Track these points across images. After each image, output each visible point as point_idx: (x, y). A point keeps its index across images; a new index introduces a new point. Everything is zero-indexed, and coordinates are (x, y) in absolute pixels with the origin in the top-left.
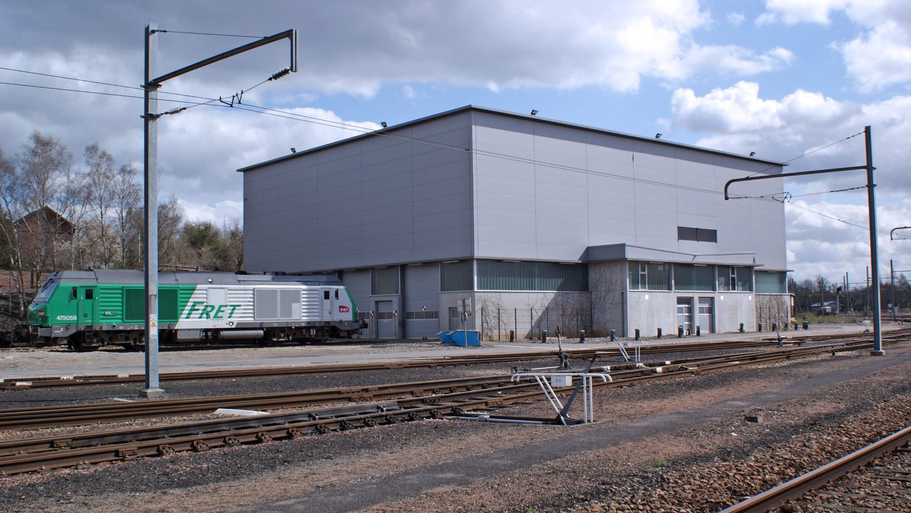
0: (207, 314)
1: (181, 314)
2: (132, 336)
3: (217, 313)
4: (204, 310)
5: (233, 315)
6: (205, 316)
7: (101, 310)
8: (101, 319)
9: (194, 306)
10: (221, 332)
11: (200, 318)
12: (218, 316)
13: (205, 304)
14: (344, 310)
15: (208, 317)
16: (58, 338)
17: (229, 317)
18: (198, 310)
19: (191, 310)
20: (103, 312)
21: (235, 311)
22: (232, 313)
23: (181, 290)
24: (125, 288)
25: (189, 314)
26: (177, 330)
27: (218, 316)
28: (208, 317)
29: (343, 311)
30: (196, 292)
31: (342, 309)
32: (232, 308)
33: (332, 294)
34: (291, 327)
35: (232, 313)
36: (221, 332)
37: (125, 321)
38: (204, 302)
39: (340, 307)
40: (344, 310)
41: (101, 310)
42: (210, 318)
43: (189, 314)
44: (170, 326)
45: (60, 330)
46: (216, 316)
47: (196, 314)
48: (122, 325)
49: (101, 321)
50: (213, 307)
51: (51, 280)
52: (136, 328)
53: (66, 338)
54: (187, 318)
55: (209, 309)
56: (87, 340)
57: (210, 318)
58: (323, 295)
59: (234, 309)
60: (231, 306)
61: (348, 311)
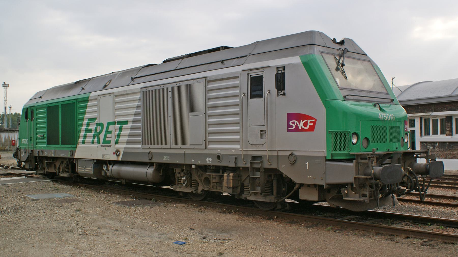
3: (105, 137)
4: (96, 130)
5: (121, 139)
9: (88, 125)
11: (93, 142)
12: (107, 139)
13: (97, 121)
14: (301, 125)
17: (117, 142)
18: (90, 131)
21: (123, 132)
22: (119, 136)
25: (85, 137)
28: (99, 142)
29: (297, 129)
30: (89, 104)
31: (294, 123)
34: (190, 166)
35: (119, 136)
39: (291, 117)
40: (301, 125)
43: (85, 137)
46: (105, 142)
54: (84, 142)
59: (121, 129)
60: (119, 123)
61: (312, 129)
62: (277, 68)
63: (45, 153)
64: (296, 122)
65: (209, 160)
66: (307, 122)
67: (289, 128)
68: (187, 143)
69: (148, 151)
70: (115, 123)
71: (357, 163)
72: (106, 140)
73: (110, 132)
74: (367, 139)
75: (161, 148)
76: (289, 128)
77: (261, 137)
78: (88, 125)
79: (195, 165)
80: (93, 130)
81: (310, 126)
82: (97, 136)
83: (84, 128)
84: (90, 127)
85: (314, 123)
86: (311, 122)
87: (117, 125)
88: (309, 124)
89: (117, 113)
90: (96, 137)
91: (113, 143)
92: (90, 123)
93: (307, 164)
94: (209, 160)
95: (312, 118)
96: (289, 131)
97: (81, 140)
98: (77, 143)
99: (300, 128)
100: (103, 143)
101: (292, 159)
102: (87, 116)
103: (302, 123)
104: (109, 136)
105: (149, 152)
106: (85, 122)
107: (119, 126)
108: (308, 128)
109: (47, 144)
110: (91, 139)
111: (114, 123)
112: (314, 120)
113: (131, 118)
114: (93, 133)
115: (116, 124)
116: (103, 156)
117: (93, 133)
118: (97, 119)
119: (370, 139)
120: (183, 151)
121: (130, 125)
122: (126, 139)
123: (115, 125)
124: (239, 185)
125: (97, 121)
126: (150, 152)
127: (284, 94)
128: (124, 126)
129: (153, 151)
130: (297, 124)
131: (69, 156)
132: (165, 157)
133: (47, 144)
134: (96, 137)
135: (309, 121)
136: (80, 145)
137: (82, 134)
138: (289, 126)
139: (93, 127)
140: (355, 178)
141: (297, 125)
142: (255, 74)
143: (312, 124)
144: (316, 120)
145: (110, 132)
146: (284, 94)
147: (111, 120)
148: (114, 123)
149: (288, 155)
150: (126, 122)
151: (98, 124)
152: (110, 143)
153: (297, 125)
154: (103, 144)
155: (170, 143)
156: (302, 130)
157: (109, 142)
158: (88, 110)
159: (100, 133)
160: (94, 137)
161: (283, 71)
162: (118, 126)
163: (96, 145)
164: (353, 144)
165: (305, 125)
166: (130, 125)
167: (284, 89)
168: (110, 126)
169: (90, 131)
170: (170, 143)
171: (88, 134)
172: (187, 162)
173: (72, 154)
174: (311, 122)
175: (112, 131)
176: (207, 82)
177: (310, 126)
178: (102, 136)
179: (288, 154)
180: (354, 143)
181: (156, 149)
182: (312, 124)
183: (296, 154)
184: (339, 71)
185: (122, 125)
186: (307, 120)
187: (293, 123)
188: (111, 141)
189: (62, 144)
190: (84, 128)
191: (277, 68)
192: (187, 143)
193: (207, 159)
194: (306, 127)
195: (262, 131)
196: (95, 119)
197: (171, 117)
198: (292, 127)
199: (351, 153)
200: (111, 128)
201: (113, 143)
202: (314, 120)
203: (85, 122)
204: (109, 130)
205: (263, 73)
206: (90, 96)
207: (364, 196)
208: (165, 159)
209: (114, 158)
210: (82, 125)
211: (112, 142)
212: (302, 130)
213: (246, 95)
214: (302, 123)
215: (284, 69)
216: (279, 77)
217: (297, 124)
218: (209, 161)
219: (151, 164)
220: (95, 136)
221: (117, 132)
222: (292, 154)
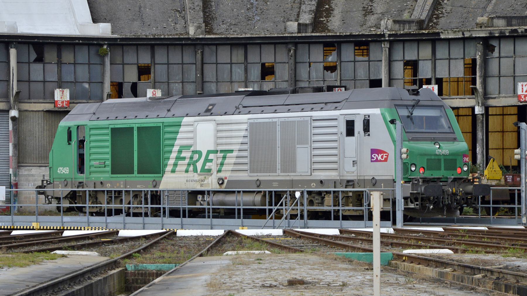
3: (204, 164)
4: (191, 158)
5: (224, 168)
9: (180, 152)
11: (187, 171)
12: (206, 168)
13: (192, 149)
17: (219, 171)
18: (184, 158)
21: (226, 161)
22: (222, 164)
25: (175, 165)
27: (206, 168)
28: (195, 170)
29: (377, 160)
31: (375, 156)
33: (359, 127)
35: (222, 164)
38: (191, 146)
39: (373, 151)
40: (379, 158)
43: (175, 165)
46: (203, 169)
47: (182, 166)
50: (200, 153)
54: (173, 171)
58: (343, 128)
59: (224, 158)
60: (222, 151)
61: (386, 160)
62: (365, 116)
63: (108, 185)
64: (376, 155)
66: (383, 155)
67: (372, 160)
68: (295, 171)
69: (256, 179)
70: (217, 151)
71: (413, 184)
73: (211, 161)
74: (424, 168)
75: (269, 176)
76: (372, 160)
77: (353, 166)
81: (385, 158)
82: (193, 165)
83: (174, 155)
84: (183, 155)
85: (387, 156)
86: (385, 156)
87: (220, 153)
88: (384, 157)
89: (220, 141)
90: (192, 166)
91: (214, 171)
92: (183, 151)
93: (382, 185)
94: (313, 185)
95: (386, 153)
96: (372, 161)
97: (169, 168)
98: (164, 172)
99: (379, 159)
100: (200, 172)
101: (374, 181)
103: (380, 156)
104: (208, 164)
105: (257, 179)
106: (176, 149)
107: (223, 154)
108: (384, 159)
109: (112, 173)
110: (184, 168)
112: (387, 154)
113: (237, 147)
115: (219, 152)
117: (187, 161)
118: (193, 146)
119: (426, 168)
122: (231, 168)
123: (217, 153)
124: (337, 204)
125: (192, 149)
126: (258, 180)
127: (369, 135)
128: (229, 155)
129: (260, 178)
130: (377, 157)
133: (112, 173)
134: (192, 166)
135: (385, 154)
137: (171, 162)
138: (372, 158)
139: (186, 154)
140: (411, 193)
141: (377, 158)
142: (350, 118)
143: (386, 157)
144: (388, 154)
145: (211, 161)
146: (369, 135)
147: (212, 148)
149: (371, 178)
150: (231, 151)
151: (194, 152)
152: (210, 172)
153: (377, 158)
155: (279, 172)
156: (380, 161)
157: (209, 170)
159: (197, 161)
160: (189, 165)
161: (368, 118)
164: (411, 170)
165: (382, 157)
166: (235, 154)
167: (369, 131)
168: (210, 154)
169: (184, 158)
170: (279, 172)
171: (180, 162)
173: (155, 185)
174: (385, 156)
175: (212, 160)
176: (312, 120)
177: (385, 158)
178: (199, 165)
179: (371, 178)
180: (413, 170)
181: (264, 177)
182: (386, 157)
183: (376, 178)
184: (409, 118)
185: (225, 154)
186: (383, 154)
187: (375, 156)
189: (138, 173)
190: (174, 155)
191: (365, 116)
192: (295, 171)
193: (312, 185)
194: (383, 159)
195: (353, 161)
196: (191, 146)
197: (280, 148)
198: (374, 158)
199: (409, 177)
200: (211, 156)
201: (214, 171)
202: (387, 154)
204: (209, 158)
205: (355, 118)
206: (183, 121)
207: (417, 205)
209: (217, 187)
210: (171, 152)
212: (380, 161)
213: (343, 133)
214: (380, 156)
215: (369, 117)
216: (365, 123)
217: (377, 157)
220: (190, 165)
221: (220, 161)
222: (373, 178)
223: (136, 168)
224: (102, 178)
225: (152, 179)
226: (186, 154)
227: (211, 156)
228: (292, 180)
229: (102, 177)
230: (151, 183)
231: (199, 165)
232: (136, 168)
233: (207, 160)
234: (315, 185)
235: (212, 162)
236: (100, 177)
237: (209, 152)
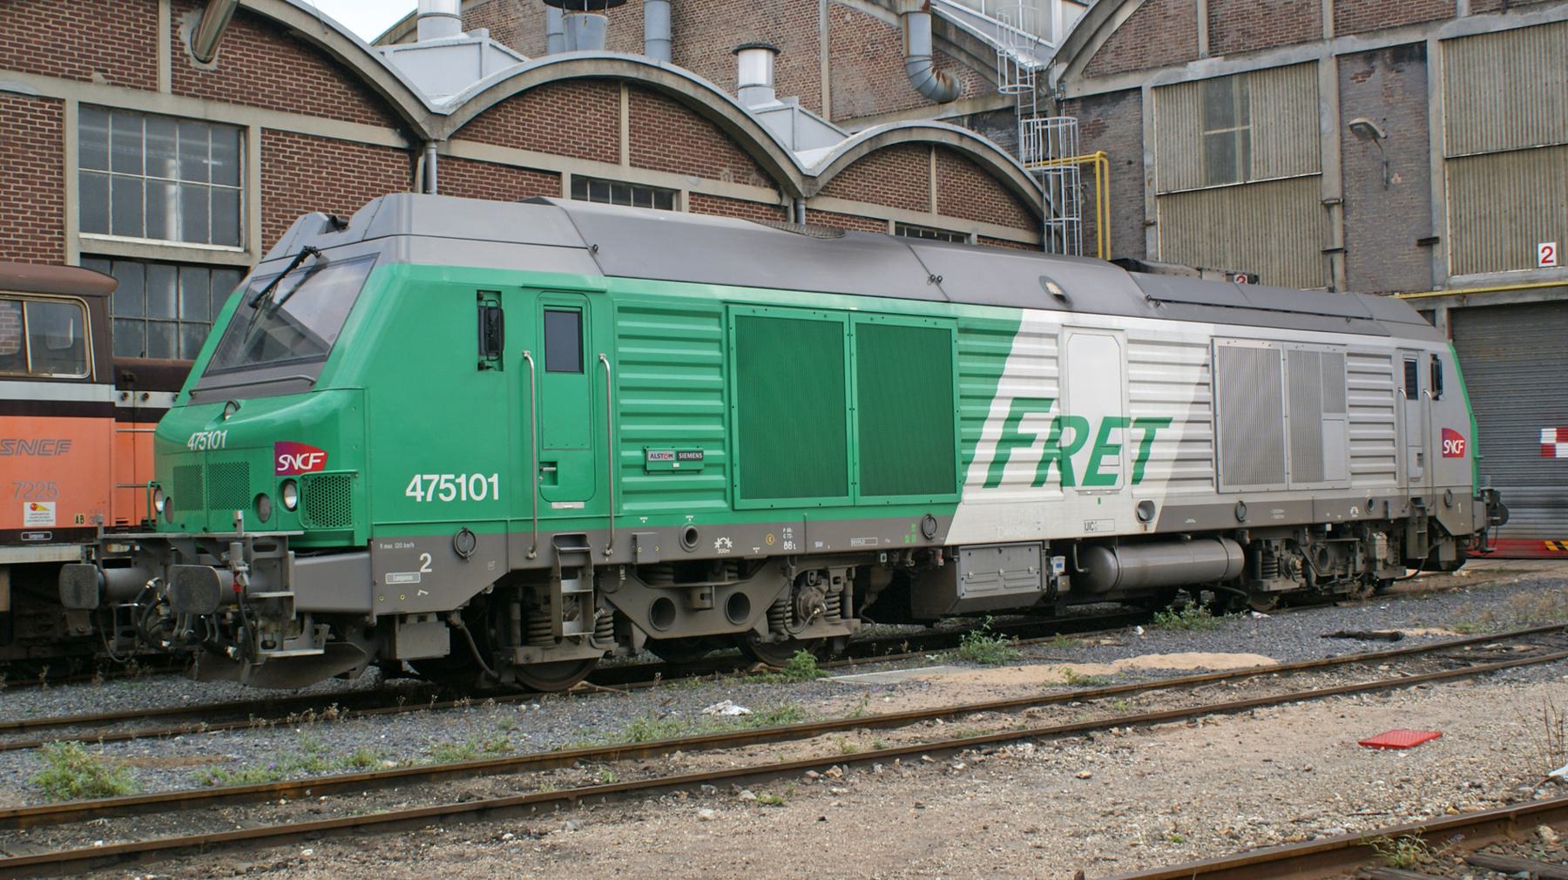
0: (1063, 465)
1: (967, 462)
2: (761, 593)
3: (1095, 462)
4: (1052, 441)
6: (1053, 472)
7: (629, 441)
8: (632, 493)
9: (1014, 419)
10: (1110, 558)
11: (1039, 482)
12: (1101, 471)
13: (1054, 411)
15: (1066, 480)
16: (403, 618)
17: (1137, 480)
18: (1028, 441)
19: (1007, 441)
20: (634, 454)
21: (1155, 450)
22: (1142, 460)
23: (965, 331)
24: (734, 310)
25: (999, 463)
26: (955, 548)
27: (1101, 471)
28: (1066, 480)
29: (1451, 455)
30: (1018, 345)
32: (1141, 432)
35: (1142, 460)
36: (1110, 558)
37: (741, 503)
40: (1454, 449)
41: (629, 441)
42: (1072, 484)
43: (999, 463)
44: (929, 528)
45: (415, 566)
46: (1092, 478)
48: (725, 531)
49: (626, 507)
50: (1081, 424)
51: (307, 252)
52: (788, 547)
53: (443, 616)
54: (992, 483)
55: (1069, 436)
56: (569, 629)
57: (1072, 484)
59: (1148, 441)
61: (1461, 455)
63: (718, 544)
65: (1354, 512)
72: (1099, 472)
73: (1115, 449)
75: (1268, 491)
78: (1014, 419)
79: (1332, 523)
80: (1040, 441)
83: (992, 430)
84: (1023, 429)
87: (1134, 427)
88: (1460, 447)
94: (1354, 512)
96: (1444, 455)
97: (976, 473)
100: (1083, 484)
102: (1005, 388)
103: (1455, 443)
104: (1105, 459)
106: (1000, 409)
110: (1031, 473)
111: (1123, 422)
114: (1037, 451)
115: (1132, 424)
116: (1088, 526)
117: (1037, 451)
118: (1055, 402)
120: (1308, 497)
121: (1176, 431)
122: (1167, 470)
125: (1054, 411)
128: (1161, 432)
129: (1247, 499)
131: (912, 539)
132: (1275, 511)
136: (968, 495)
137: (985, 452)
145: (1115, 449)
148: (1123, 422)
150: (1166, 422)
151: (1059, 422)
152: (1113, 484)
154: (1083, 484)
155: (1289, 478)
156: (1455, 455)
157: (1110, 479)
158: (1010, 366)
160: (1044, 463)
162: (1141, 432)
163: (1051, 492)
166: (1176, 431)
168: (1112, 429)
169: (1028, 441)
170: (1289, 478)
171: (1016, 452)
172: (1319, 520)
175: (1118, 447)
178: (1080, 462)
181: (1255, 495)
188: (1115, 476)
189: (865, 492)
190: (992, 430)
193: (1352, 511)
195: (1419, 455)
200: (1115, 436)
203: (1000, 409)
204: (1108, 442)
208: (1277, 517)
211: (1119, 481)
212: (1455, 455)
218: (1355, 513)
219: (1231, 534)
223: (854, 472)
224: (689, 517)
225: (921, 513)
226: (1037, 426)
227: (1115, 436)
228: (1313, 501)
229: (691, 511)
230: (914, 526)
231: (1080, 462)
232: (854, 472)
233: (1103, 447)
234: (1357, 511)
235: (1118, 454)
236: (681, 513)
237: (1108, 424)
